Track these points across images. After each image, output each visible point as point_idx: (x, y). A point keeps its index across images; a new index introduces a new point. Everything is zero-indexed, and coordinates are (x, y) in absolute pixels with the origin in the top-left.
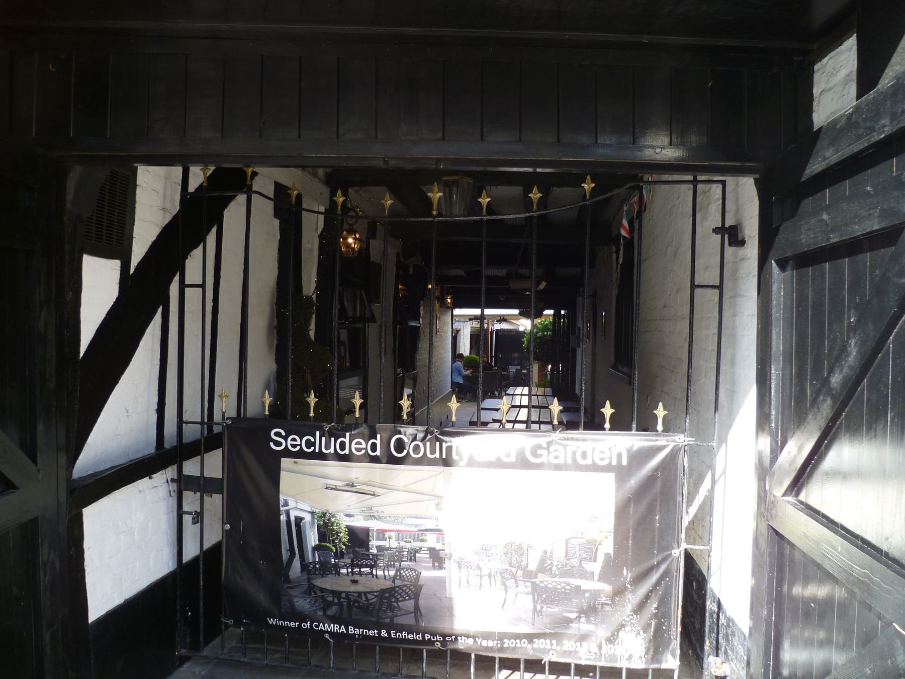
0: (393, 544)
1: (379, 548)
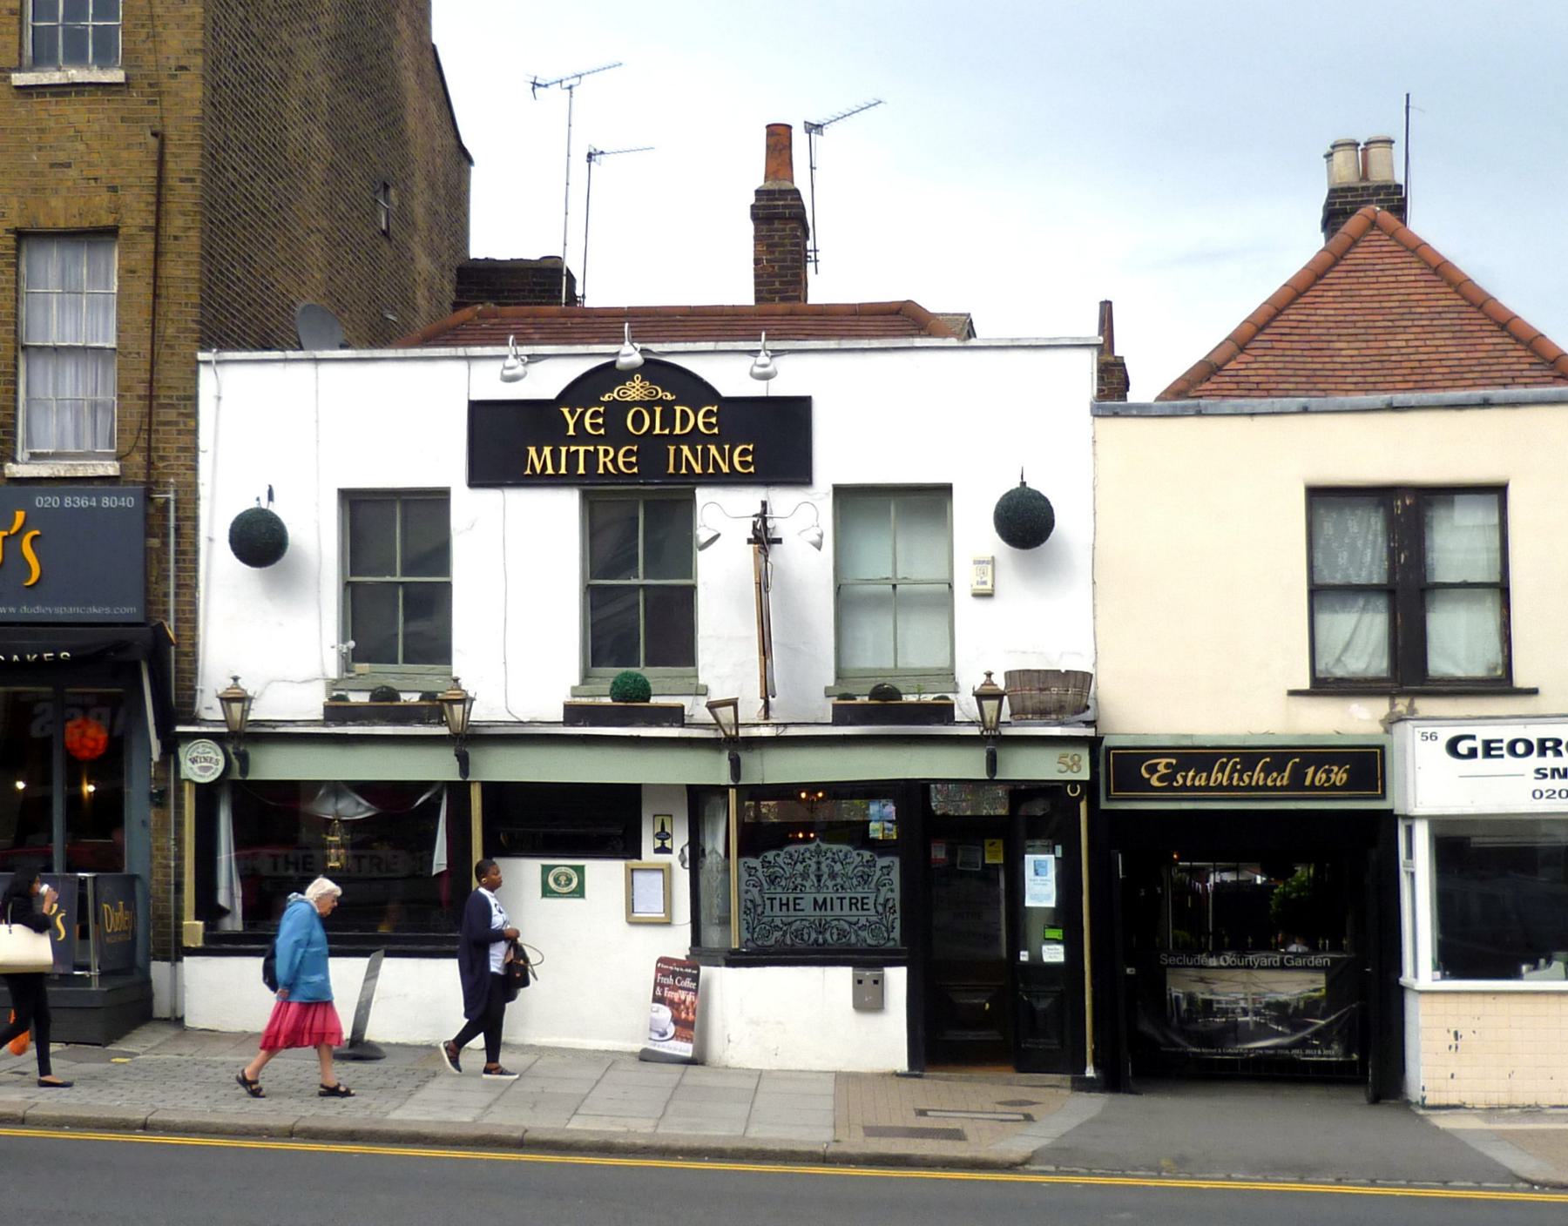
0: (1224, 1006)
1: (1218, 1008)
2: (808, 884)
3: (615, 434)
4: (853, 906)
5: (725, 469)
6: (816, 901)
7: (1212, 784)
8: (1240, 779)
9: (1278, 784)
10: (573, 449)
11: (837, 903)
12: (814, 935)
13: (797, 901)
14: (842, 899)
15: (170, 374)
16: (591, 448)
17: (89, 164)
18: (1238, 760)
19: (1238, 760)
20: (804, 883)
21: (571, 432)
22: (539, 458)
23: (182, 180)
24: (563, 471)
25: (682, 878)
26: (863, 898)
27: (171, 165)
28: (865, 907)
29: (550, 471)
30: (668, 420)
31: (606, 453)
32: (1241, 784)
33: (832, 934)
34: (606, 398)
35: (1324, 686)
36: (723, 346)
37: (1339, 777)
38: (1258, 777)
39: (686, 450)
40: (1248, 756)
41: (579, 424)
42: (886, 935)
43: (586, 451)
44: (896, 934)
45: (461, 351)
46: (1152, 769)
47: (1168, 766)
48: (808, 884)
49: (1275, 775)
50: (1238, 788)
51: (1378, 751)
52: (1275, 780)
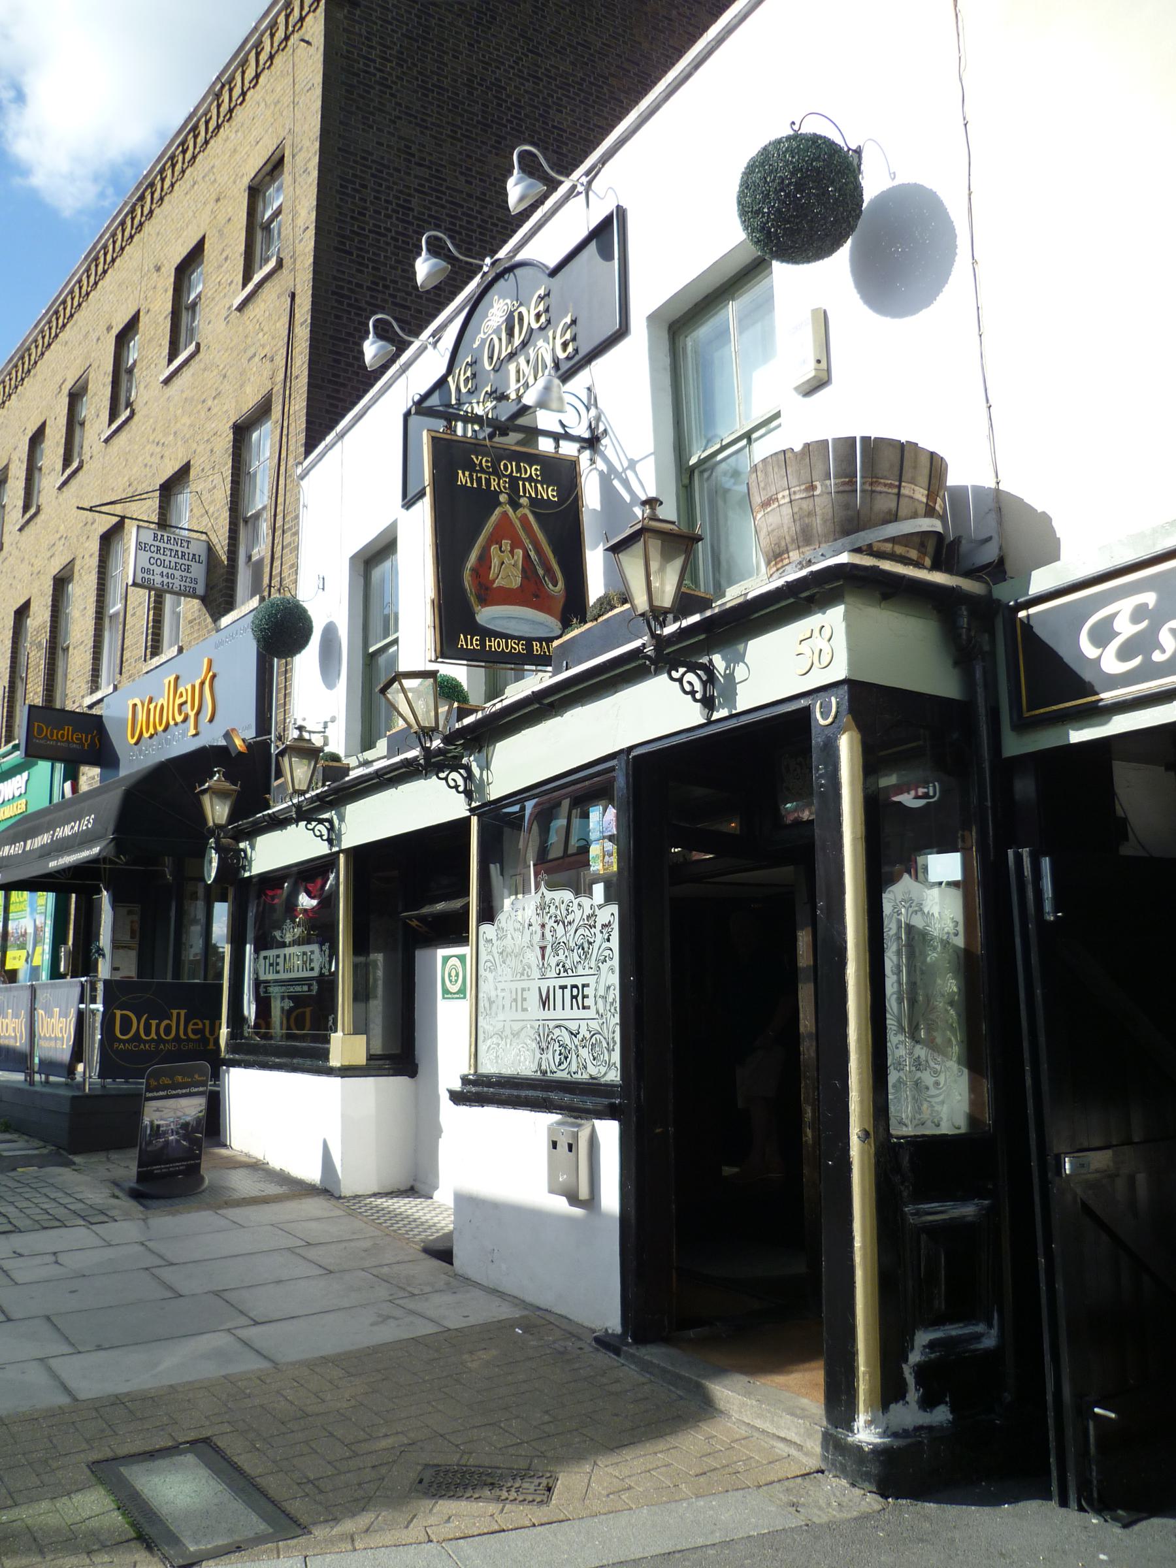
14: (563, 988)
26: (584, 986)
46: (1102, 635)
47: (1138, 614)
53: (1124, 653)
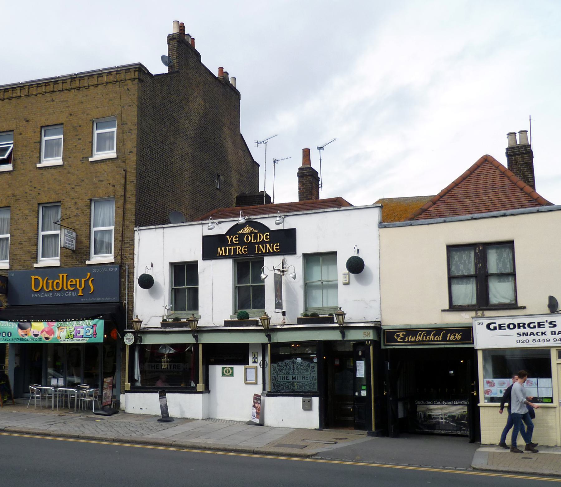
2: (290, 372)
3: (241, 243)
4: (303, 379)
5: (271, 251)
6: (292, 377)
7: (417, 340)
8: (426, 338)
9: (438, 340)
10: (230, 247)
11: (299, 378)
12: (292, 387)
13: (287, 377)
14: (300, 376)
15: (127, 234)
16: (235, 247)
17: (108, 180)
18: (425, 332)
19: (425, 332)
20: (289, 371)
21: (229, 243)
22: (221, 251)
23: (131, 182)
24: (227, 254)
25: (260, 370)
27: (128, 178)
28: (307, 379)
29: (224, 254)
30: (255, 238)
31: (239, 248)
32: (426, 340)
33: (297, 387)
34: (239, 233)
35: (453, 308)
36: (270, 215)
37: (458, 337)
38: (432, 337)
39: (261, 246)
40: (428, 331)
41: (232, 240)
42: (313, 387)
43: (233, 248)
44: (316, 387)
45: (200, 222)
46: (398, 336)
48: (290, 372)
49: (437, 337)
50: (425, 341)
51: (471, 328)
52: (437, 338)
53: (401, 339)
